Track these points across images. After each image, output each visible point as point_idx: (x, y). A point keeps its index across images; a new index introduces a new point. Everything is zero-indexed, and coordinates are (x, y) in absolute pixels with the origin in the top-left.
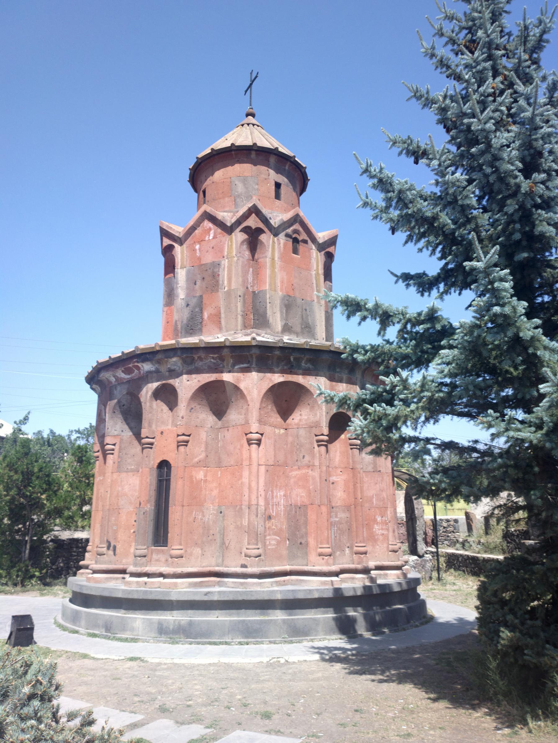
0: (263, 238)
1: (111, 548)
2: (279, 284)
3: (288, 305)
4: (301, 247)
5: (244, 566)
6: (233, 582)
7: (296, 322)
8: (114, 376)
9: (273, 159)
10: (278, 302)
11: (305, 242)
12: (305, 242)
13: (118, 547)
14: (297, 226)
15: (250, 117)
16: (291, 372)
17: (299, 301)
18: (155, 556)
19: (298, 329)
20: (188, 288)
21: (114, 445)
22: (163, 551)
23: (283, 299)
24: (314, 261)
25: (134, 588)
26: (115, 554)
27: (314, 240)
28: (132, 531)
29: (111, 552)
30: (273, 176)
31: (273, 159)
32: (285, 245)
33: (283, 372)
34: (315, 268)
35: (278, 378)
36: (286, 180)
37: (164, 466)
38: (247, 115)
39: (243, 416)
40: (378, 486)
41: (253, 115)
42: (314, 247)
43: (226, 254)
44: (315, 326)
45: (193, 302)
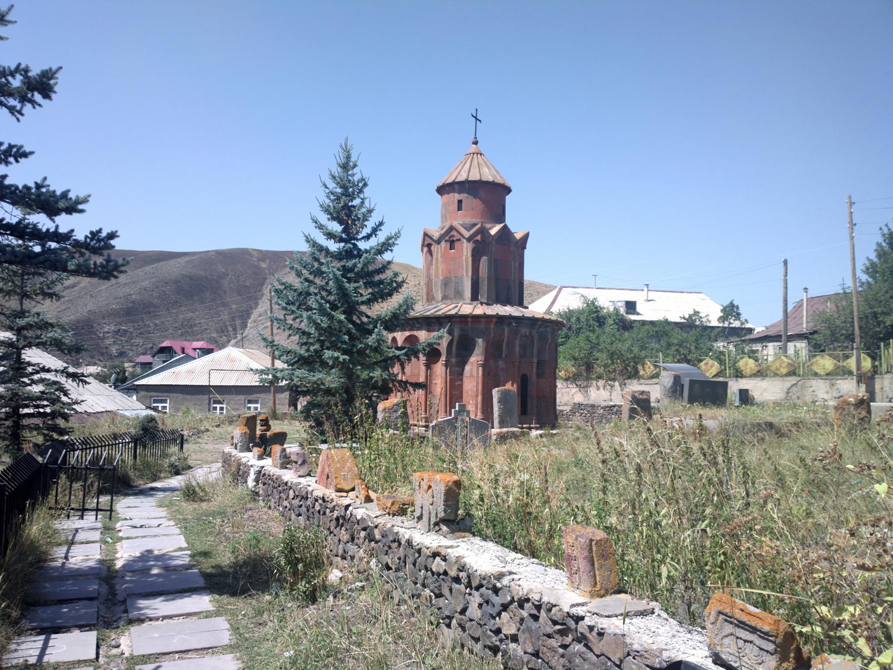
0: (432, 248)
2: (440, 272)
3: (446, 283)
4: (457, 244)
7: (451, 292)
9: (456, 187)
10: (439, 283)
11: (459, 240)
12: (459, 240)
14: (454, 233)
16: (412, 330)
17: (453, 279)
19: (452, 296)
23: (442, 281)
24: (465, 250)
27: (463, 237)
30: (457, 196)
31: (456, 187)
32: (445, 247)
33: (410, 330)
35: (407, 334)
36: (466, 195)
44: (463, 291)
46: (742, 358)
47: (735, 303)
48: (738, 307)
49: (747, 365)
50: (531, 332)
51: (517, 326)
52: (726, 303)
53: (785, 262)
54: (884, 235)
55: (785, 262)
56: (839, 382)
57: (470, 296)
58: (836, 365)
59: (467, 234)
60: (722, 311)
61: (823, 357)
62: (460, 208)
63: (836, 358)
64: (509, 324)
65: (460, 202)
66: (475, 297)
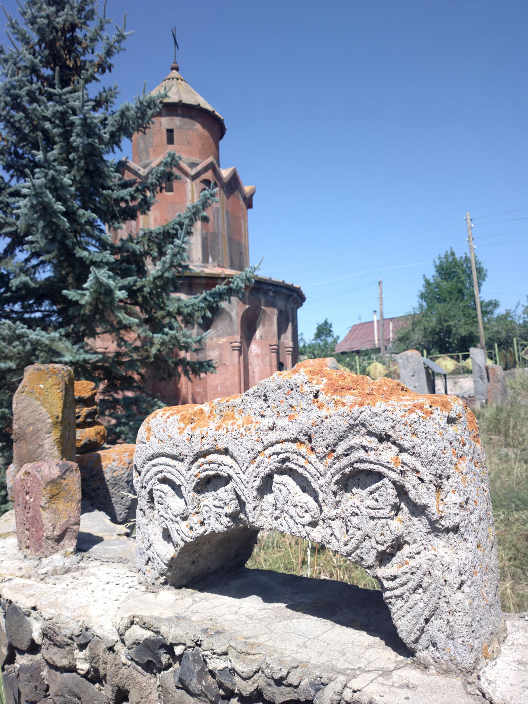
15: (174, 71)
27: (186, 174)
34: (190, 198)
38: (172, 69)
40: (222, 376)
41: (177, 69)
42: (188, 180)
46: (369, 364)
47: (329, 322)
48: (331, 326)
49: (376, 369)
50: (286, 307)
51: (274, 297)
52: (321, 322)
53: (380, 283)
54: (436, 266)
55: (380, 283)
56: (461, 380)
57: (200, 256)
58: (456, 365)
59: (193, 172)
60: (318, 328)
61: (444, 358)
62: (170, 141)
63: (457, 359)
64: (266, 293)
65: (170, 132)
66: (205, 260)
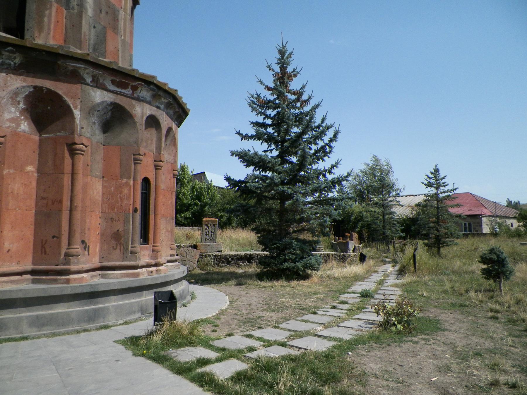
1: (87, 249)
5: (172, 255)
6: (171, 266)
8: (93, 77)
13: (90, 247)
18: (143, 252)
20: (94, 10)
21: (86, 147)
22: (147, 248)
25: (146, 276)
26: (89, 254)
28: (98, 232)
29: (86, 253)
37: (146, 181)
39: (172, 158)
43: (123, 7)
45: (99, 27)
